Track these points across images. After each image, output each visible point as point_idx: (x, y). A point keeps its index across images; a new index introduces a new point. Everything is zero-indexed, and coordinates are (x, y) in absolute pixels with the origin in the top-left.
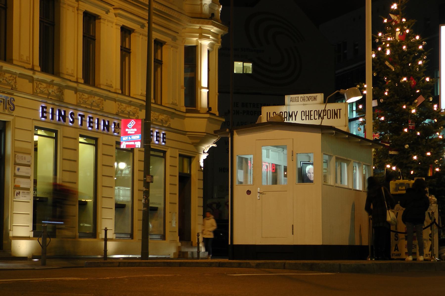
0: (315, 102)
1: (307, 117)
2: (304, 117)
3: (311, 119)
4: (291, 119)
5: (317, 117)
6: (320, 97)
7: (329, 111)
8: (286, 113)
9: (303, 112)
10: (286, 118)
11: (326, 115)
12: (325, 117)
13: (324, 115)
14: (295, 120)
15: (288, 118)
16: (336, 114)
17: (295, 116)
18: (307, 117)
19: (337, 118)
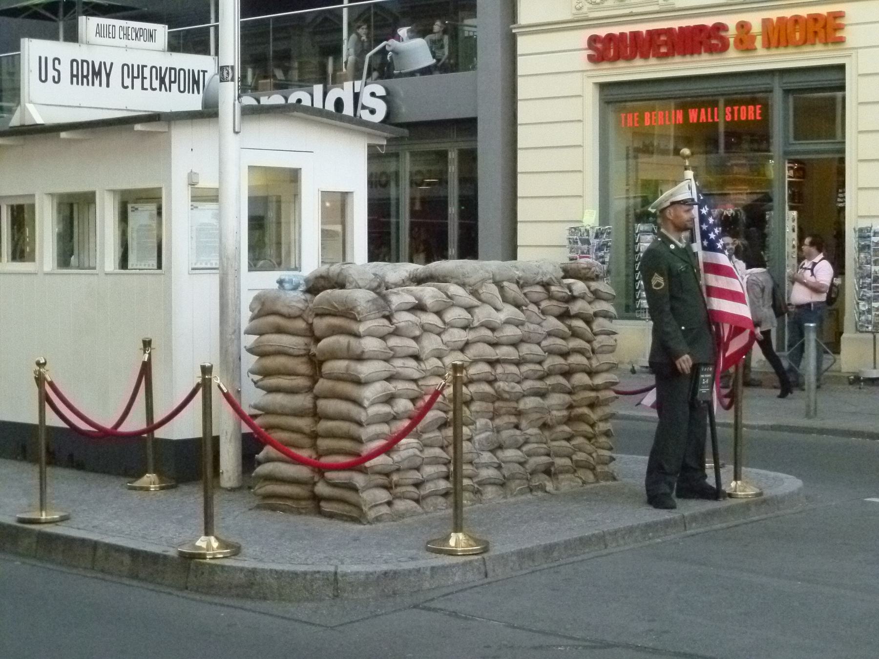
0: (149, 45)
2: (128, 82)
3: (143, 88)
4: (97, 82)
5: (156, 84)
7: (182, 72)
8: (85, 64)
9: (126, 67)
10: (87, 77)
11: (175, 82)
12: (174, 86)
13: (171, 82)
14: (108, 86)
15: (90, 78)
16: (196, 82)
17: (108, 75)
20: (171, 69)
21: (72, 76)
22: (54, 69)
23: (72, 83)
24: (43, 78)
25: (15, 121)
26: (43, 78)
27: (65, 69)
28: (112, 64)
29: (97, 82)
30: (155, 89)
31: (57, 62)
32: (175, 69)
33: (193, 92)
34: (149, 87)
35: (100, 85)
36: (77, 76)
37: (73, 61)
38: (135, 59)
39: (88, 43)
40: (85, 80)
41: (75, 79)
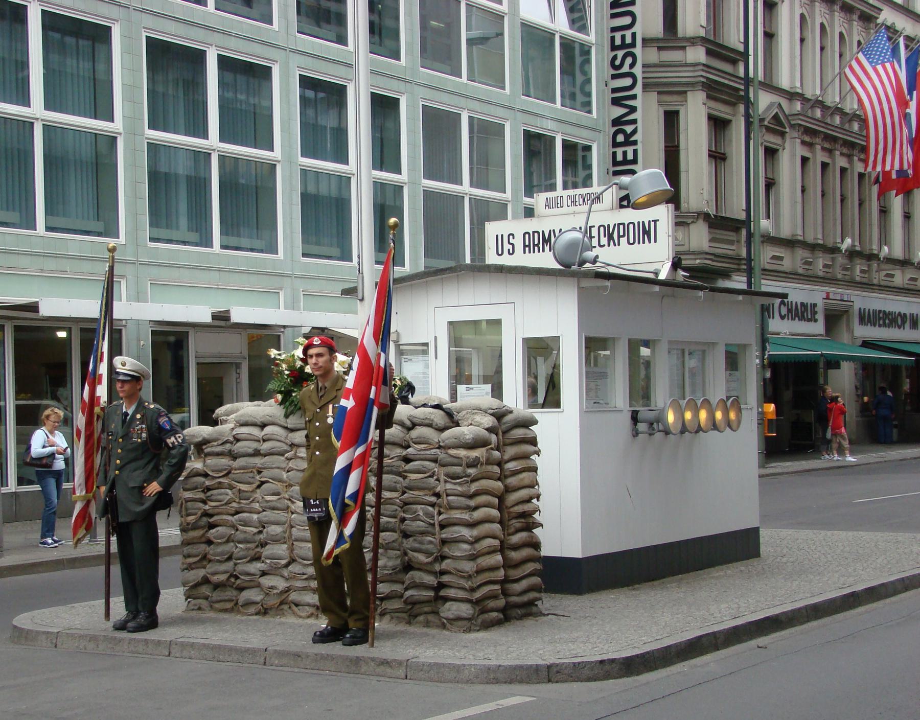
5: (604, 241)
7: (631, 226)
8: (536, 235)
10: (538, 245)
11: (624, 236)
12: (624, 240)
13: (619, 237)
15: (541, 246)
16: (647, 233)
19: (650, 242)
20: (619, 224)
21: (525, 246)
22: (509, 243)
27: (518, 242)
29: (547, 248)
32: (624, 224)
33: (644, 242)
36: (529, 246)
37: (524, 234)
40: (536, 248)
41: (527, 249)
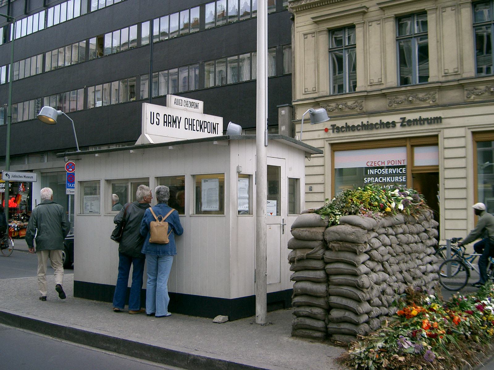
1: (190, 126)
2: (187, 127)
3: (193, 130)
4: (174, 126)
5: (199, 128)
6: (201, 104)
7: (209, 123)
8: (170, 117)
9: (186, 120)
10: (170, 123)
11: (206, 128)
12: (206, 130)
13: (204, 128)
15: (172, 123)
16: (214, 129)
17: (179, 123)
18: (190, 126)
20: (205, 122)
21: (164, 122)
23: (164, 126)
24: (152, 122)
25: (139, 142)
26: (152, 122)
27: (161, 118)
28: (181, 117)
29: (174, 126)
30: (198, 131)
31: (158, 115)
32: (206, 122)
34: (196, 130)
35: (176, 127)
36: (166, 122)
38: (191, 116)
39: (171, 107)
40: (170, 124)
41: (165, 124)
